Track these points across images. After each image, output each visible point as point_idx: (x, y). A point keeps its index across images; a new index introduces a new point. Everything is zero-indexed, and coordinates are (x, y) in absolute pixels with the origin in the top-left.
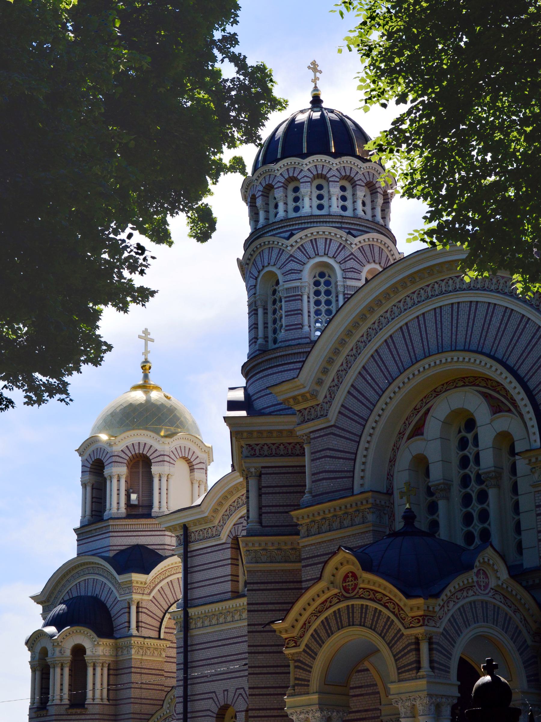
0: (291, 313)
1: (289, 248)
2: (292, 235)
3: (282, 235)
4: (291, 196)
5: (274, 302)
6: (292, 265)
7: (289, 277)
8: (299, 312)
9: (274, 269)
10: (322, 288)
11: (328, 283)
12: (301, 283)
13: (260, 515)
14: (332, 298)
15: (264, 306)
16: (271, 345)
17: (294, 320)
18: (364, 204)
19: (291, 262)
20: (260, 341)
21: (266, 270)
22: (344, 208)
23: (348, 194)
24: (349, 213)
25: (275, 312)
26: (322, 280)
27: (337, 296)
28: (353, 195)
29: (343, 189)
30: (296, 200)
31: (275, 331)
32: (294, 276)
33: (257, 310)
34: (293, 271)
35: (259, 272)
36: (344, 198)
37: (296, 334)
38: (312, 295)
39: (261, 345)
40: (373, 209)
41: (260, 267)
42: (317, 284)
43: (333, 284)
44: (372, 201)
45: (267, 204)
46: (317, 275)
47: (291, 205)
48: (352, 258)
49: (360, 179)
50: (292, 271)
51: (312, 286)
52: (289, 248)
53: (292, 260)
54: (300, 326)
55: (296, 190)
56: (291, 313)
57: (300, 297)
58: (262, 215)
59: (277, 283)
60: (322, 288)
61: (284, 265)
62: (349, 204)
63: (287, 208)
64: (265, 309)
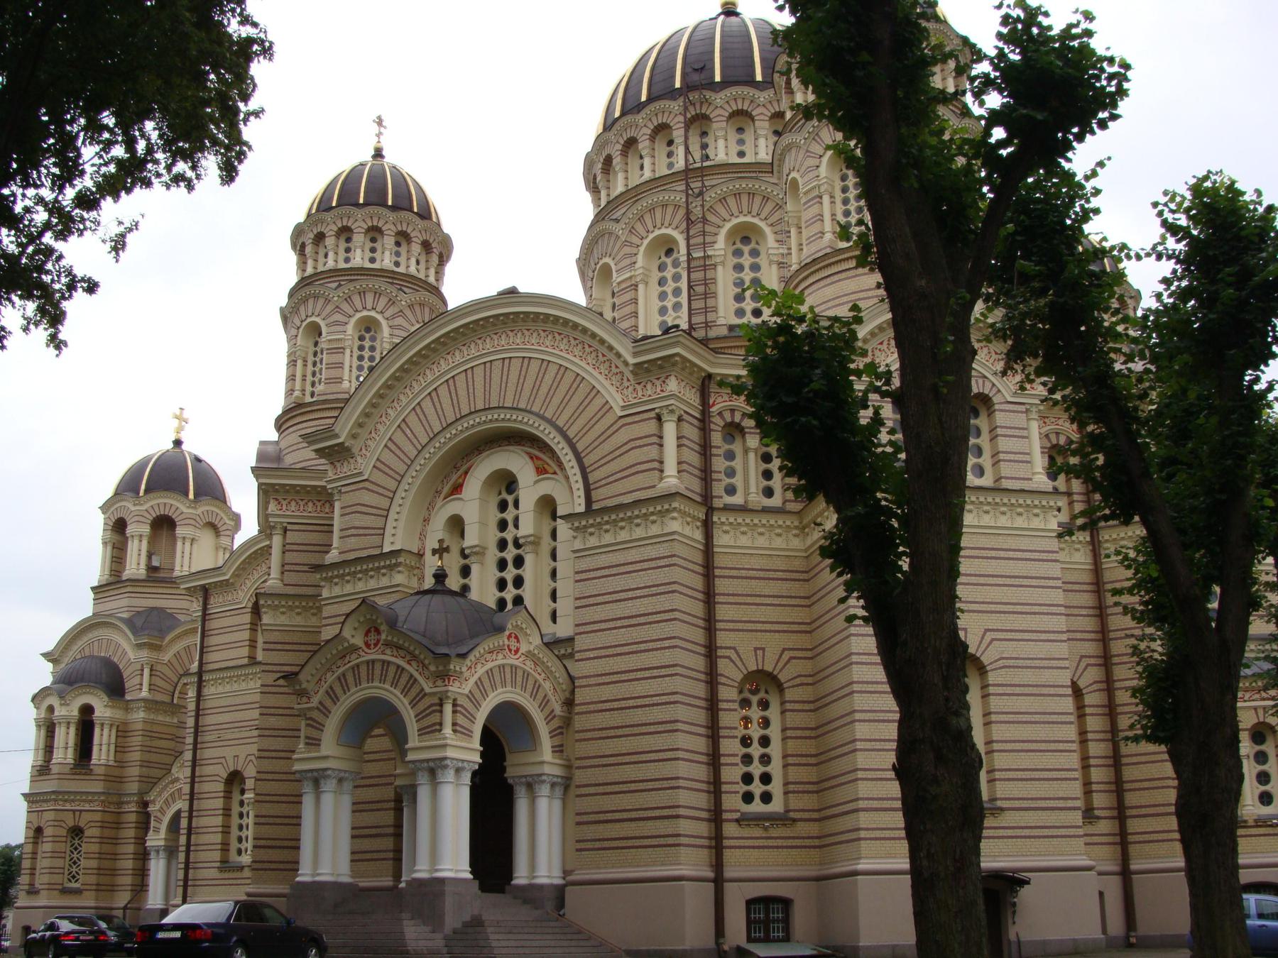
0: (331, 366)
1: (336, 299)
2: (340, 285)
3: (329, 285)
4: (343, 245)
5: (315, 354)
6: (338, 317)
7: (333, 329)
8: (340, 365)
9: (318, 320)
11: (373, 339)
13: (282, 573)
16: (308, 399)
18: (418, 262)
20: (297, 393)
21: (309, 320)
22: (397, 264)
23: (403, 250)
24: (401, 269)
25: (315, 364)
26: (367, 336)
29: (398, 244)
30: (348, 250)
31: (313, 384)
36: (398, 254)
37: (334, 388)
38: (355, 349)
39: (297, 397)
40: (427, 269)
41: (304, 317)
42: (361, 338)
43: (378, 341)
44: (427, 261)
45: (317, 253)
47: (342, 255)
50: (337, 323)
51: (357, 339)
55: (348, 240)
56: (331, 366)
58: (310, 263)
59: (320, 334)
60: (367, 344)
61: (329, 316)
62: (402, 260)
64: (305, 361)
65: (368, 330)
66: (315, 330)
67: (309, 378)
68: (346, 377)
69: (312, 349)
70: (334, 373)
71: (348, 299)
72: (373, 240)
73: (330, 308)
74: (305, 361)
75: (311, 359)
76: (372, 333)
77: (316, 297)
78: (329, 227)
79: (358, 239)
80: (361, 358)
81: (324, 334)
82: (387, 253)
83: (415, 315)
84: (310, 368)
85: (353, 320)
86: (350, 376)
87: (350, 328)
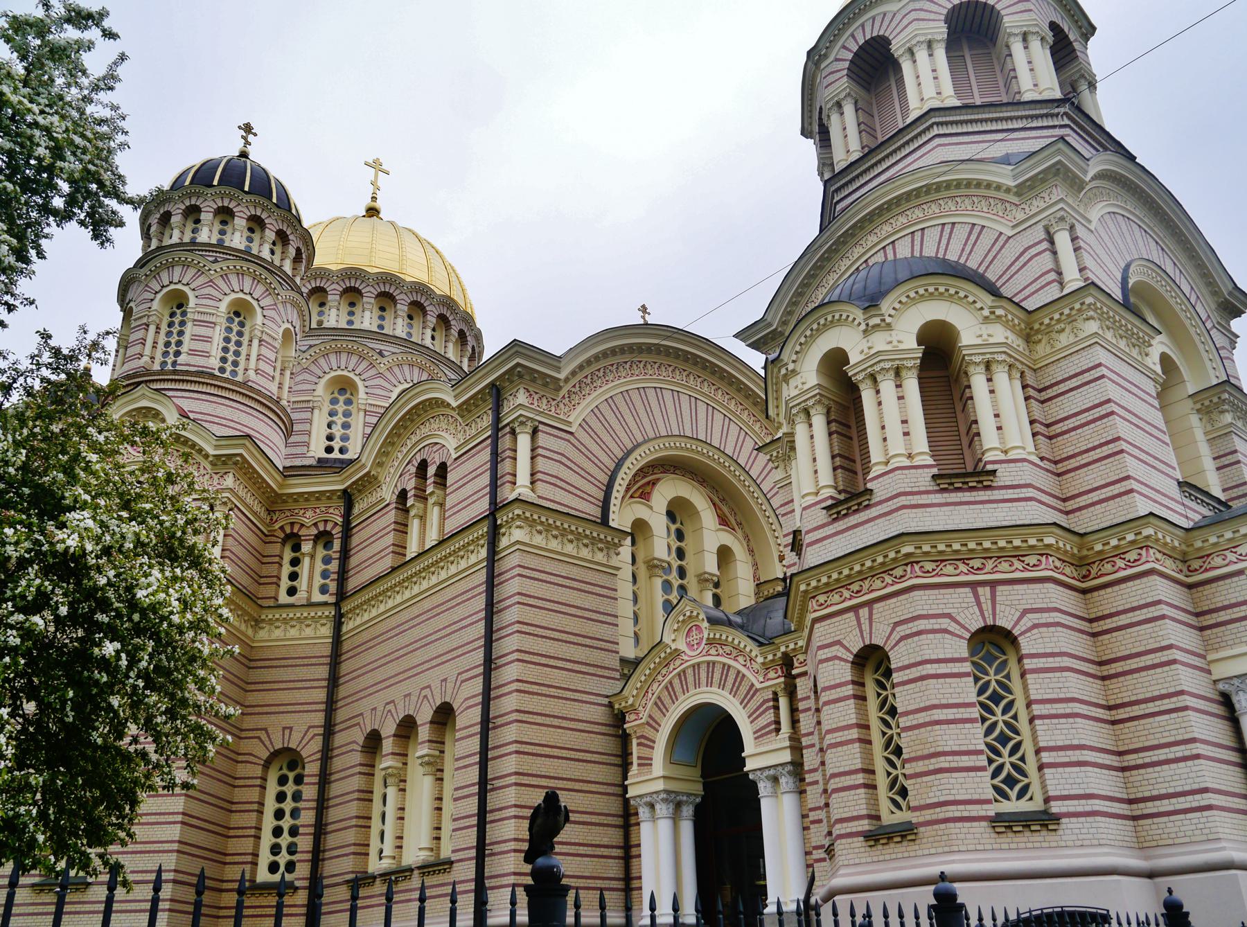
0: (195, 338)
1: (212, 272)
8: (208, 339)
10: (236, 328)
11: (242, 324)
14: (245, 340)
20: (146, 359)
26: (237, 320)
27: (251, 341)
28: (283, 253)
33: (148, 326)
35: (171, 282)
36: (272, 252)
42: (230, 320)
50: (210, 297)
52: (212, 272)
56: (195, 338)
59: (180, 306)
61: (201, 287)
64: (158, 328)
65: (237, 314)
66: (178, 302)
67: (161, 346)
68: (213, 353)
69: (166, 319)
70: (199, 346)
71: (224, 277)
72: (251, 230)
73: (202, 280)
76: (241, 318)
77: (186, 265)
78: (207, 203)
79: (240, 222)
80: (227, 340)
83: (286, 314)
84: (162, 339)
87: (223, 306)
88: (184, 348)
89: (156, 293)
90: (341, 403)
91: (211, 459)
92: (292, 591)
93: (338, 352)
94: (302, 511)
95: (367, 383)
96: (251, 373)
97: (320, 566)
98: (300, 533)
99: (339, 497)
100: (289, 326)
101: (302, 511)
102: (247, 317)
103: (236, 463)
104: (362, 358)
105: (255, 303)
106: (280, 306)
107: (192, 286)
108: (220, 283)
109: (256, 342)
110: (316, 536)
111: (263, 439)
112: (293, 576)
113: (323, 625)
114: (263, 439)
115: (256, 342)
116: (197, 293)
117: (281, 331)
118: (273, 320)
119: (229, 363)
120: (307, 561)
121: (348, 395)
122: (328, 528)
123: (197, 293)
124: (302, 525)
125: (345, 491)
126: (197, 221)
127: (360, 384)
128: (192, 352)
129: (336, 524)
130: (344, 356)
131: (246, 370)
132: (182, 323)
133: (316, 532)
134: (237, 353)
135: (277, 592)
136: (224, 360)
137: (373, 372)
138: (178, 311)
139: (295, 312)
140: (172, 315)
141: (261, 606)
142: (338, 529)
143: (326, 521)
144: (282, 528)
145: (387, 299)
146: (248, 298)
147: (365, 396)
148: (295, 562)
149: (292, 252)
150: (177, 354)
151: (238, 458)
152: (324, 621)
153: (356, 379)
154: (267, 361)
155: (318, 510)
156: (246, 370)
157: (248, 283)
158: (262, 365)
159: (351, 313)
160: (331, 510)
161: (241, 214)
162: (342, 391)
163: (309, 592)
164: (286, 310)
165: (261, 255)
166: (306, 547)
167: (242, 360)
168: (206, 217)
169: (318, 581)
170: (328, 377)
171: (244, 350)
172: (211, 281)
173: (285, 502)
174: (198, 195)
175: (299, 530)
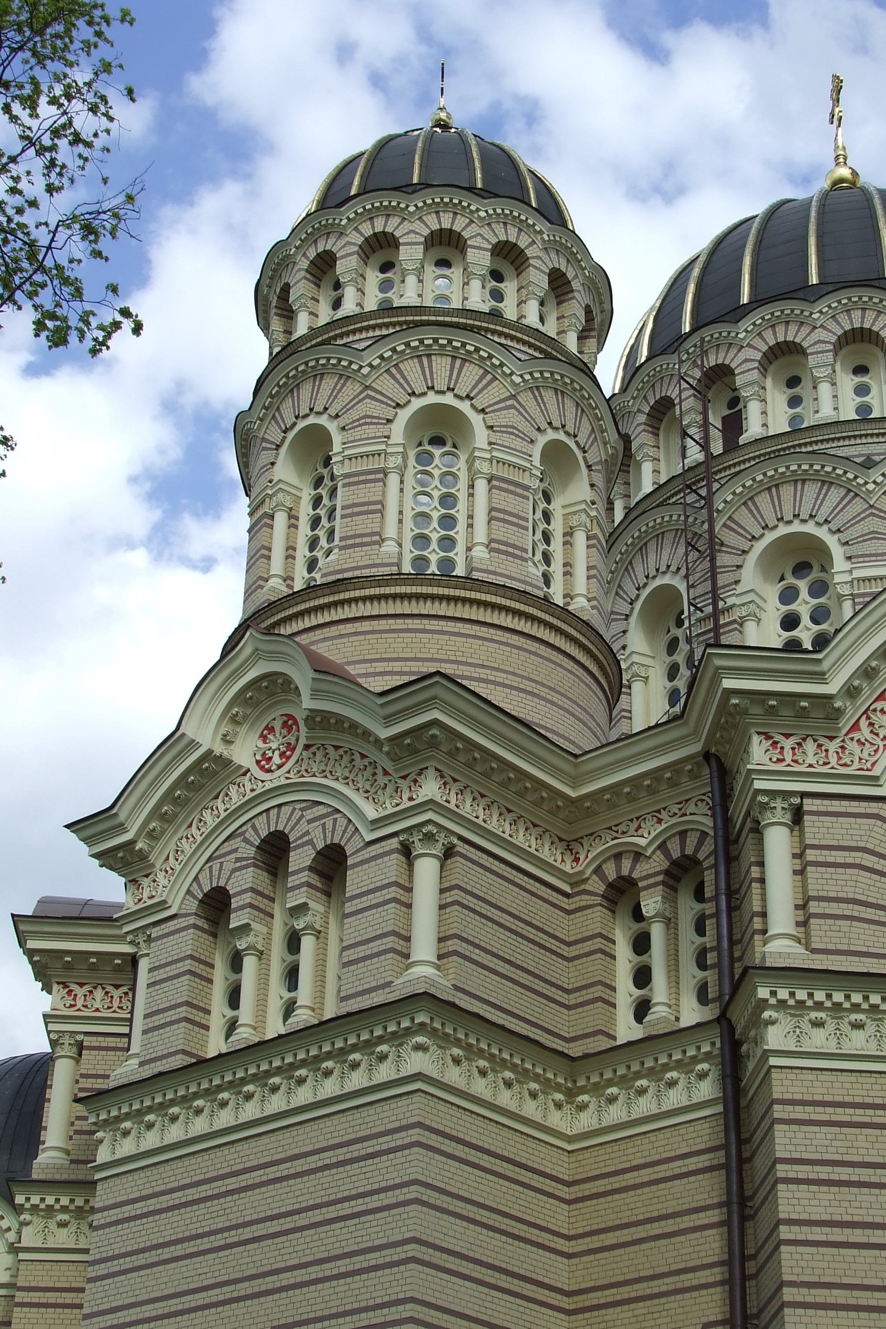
0: (353, 510)
5: (317, 502)
7: (358, 433)
12: (387, 445)
14: (461, 490)
15: (291, 509)
17: (365, 524)
19: (368, 401)
25: (315, 522)
27: (472, 486)
32: (371, 430)
33: (272, 517)
34: (368, 420)
36: (497, 296)
46: (426, 442)
48: (512, 407)
49: (538, 257)
50: (367, 420)
53: (368, 396)
54: (377, 538)
56: (353, 510)
57: (381, 476)
59: (327, 462)
63: (362, 299)
64: (292, 517)
67: (302, 552)
68: (391, 531)
74: (292, 517)
75: (305, 511)
77: (318, 374)
81: (337, 447)
82: (476, 284)
83: (545, 410)
85: (404, 416)
86: (400, 532)
87: (398, 431)
88: (337, 542)
89: (278, 447)
90: (804, 594)
91: (386, 749)
92: (642, 1009)
93: (773, 486)
94: (635, 824)
95: (844, 537)
96: (480, 552)
97: (689, 941)
98: (635, 875)
99: (694, 775)
100: (561, 436)
101: (635, 824)
102: (459, 444)
103: (434, 743)
104: (827, 483)
105: (464, 407)
106: (526, 399)
107: (332, 411)
108: (385, 385)
109: (481, 485)
110: (667, 873)
111: (483, 673)
112: (642, 977)
113: (702, 1076)
114: (483, 673)
115: (481, 485)
116: (341, 422)
117: (537, 452)
118: (511, 430)
119: (434, 545)
120: (657, 932)
121: (815, 574)
122: (689, 851)
123: (341, 422)
124: (638, 855)
125: (707, 756)
126: (337, 286)
127: (832, 542)
128: (352, 543)
129: (704, 834)
130: (787, 491)
131: (469, 549)
132: (333, 492)
133: (666, 864)
134: (448, 521)
135: (612, 1020)
136: (422, 540)
137: (858, 506)
138: (325, 472)
139: (569, 404)
140: (318, 483)
141: (573, 1059)
142: (709, 846)
143: (683, 834)
144: (598, 871)
145: (865, 346)
146: (448, 399)
147: (847, 566)
148: (641, 944)
149: (539, 280)
150: (328, 553)
151: (435, 731)
152: (705, 1066)
153: (822, 533)
154: (517, 521)
155: (664, 815)
156: (469, 549)
157: (441, 366)
158: (502, 532)
159: (795, 402)
160: (691, 808)
161: (412, 238)
162: (801, 569)
163: (674, 1005)
164: (541, 403)
165: (470, 305)
166: (651, 904)
167: (460, 533)
168: (346, 266)
169: (691, 974)
170: (760, 546)
171: (460, 512)
172: (367, 387)
173: (590, 813)
174: (328, 231)
175: (632, 869)
